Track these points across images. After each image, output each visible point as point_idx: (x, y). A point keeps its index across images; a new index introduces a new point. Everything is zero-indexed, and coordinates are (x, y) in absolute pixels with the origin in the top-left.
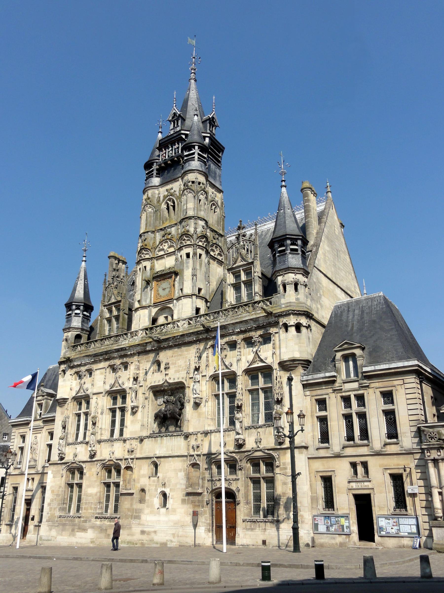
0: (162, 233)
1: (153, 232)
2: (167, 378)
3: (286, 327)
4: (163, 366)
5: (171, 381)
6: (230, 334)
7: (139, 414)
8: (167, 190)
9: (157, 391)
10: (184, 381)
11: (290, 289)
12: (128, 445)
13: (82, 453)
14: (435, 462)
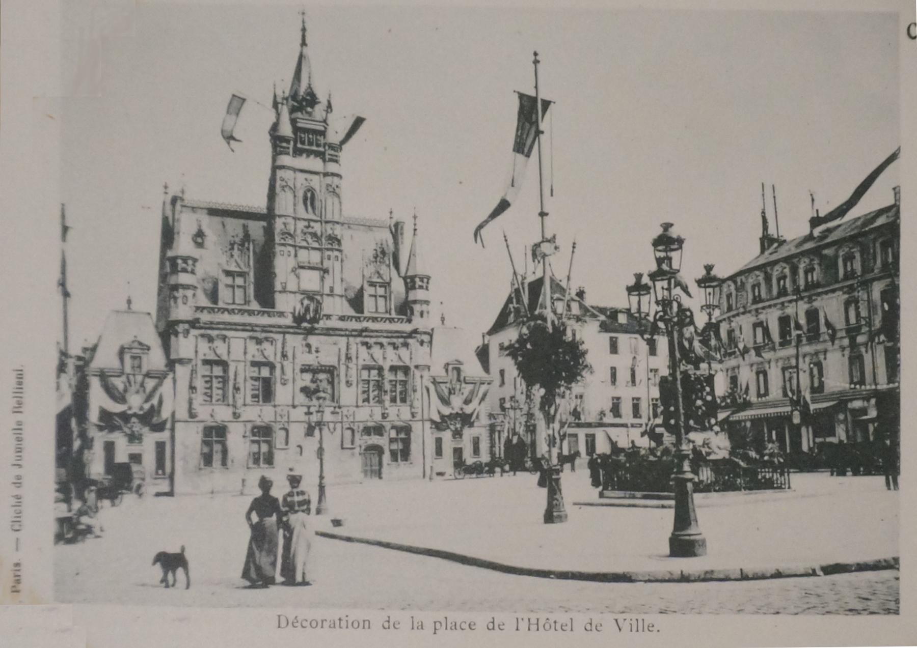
0: (306, 223)
1: (295, 218)
2: (319, 359)
3: (422, 343)
4: (313, 349)
5: (323, 363)
6: (377, 337)
7: (290, 385)
8: (306, 179)
9: (305, 369)
10: (336, 365)
11: (425, 314)
12: (278, 409)
13: (223, 414)
14: (499, 432)
